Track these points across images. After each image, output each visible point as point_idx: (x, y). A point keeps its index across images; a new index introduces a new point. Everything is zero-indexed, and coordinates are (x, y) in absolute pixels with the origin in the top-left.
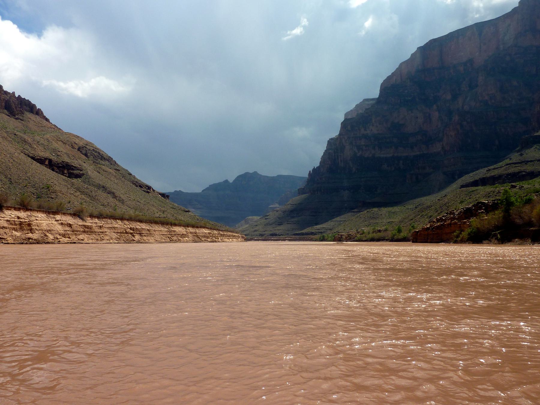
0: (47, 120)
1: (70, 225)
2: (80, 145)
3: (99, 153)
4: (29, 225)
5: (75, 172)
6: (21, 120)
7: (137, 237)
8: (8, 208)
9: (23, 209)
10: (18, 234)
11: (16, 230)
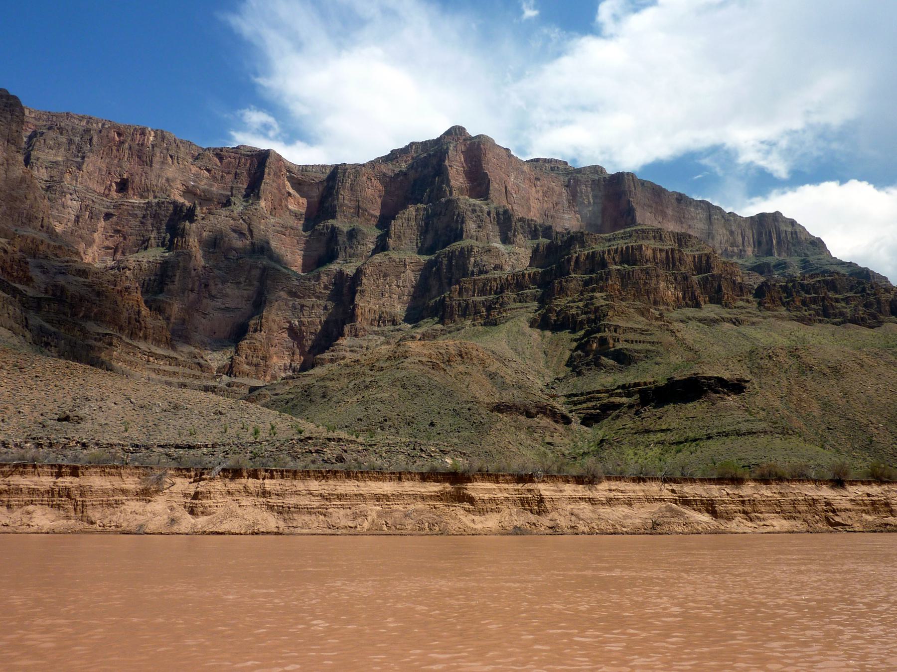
4: (887, 504)
8: (853, 483)
9: (875, 482)
10: (870, 518)
11: (868, 513)
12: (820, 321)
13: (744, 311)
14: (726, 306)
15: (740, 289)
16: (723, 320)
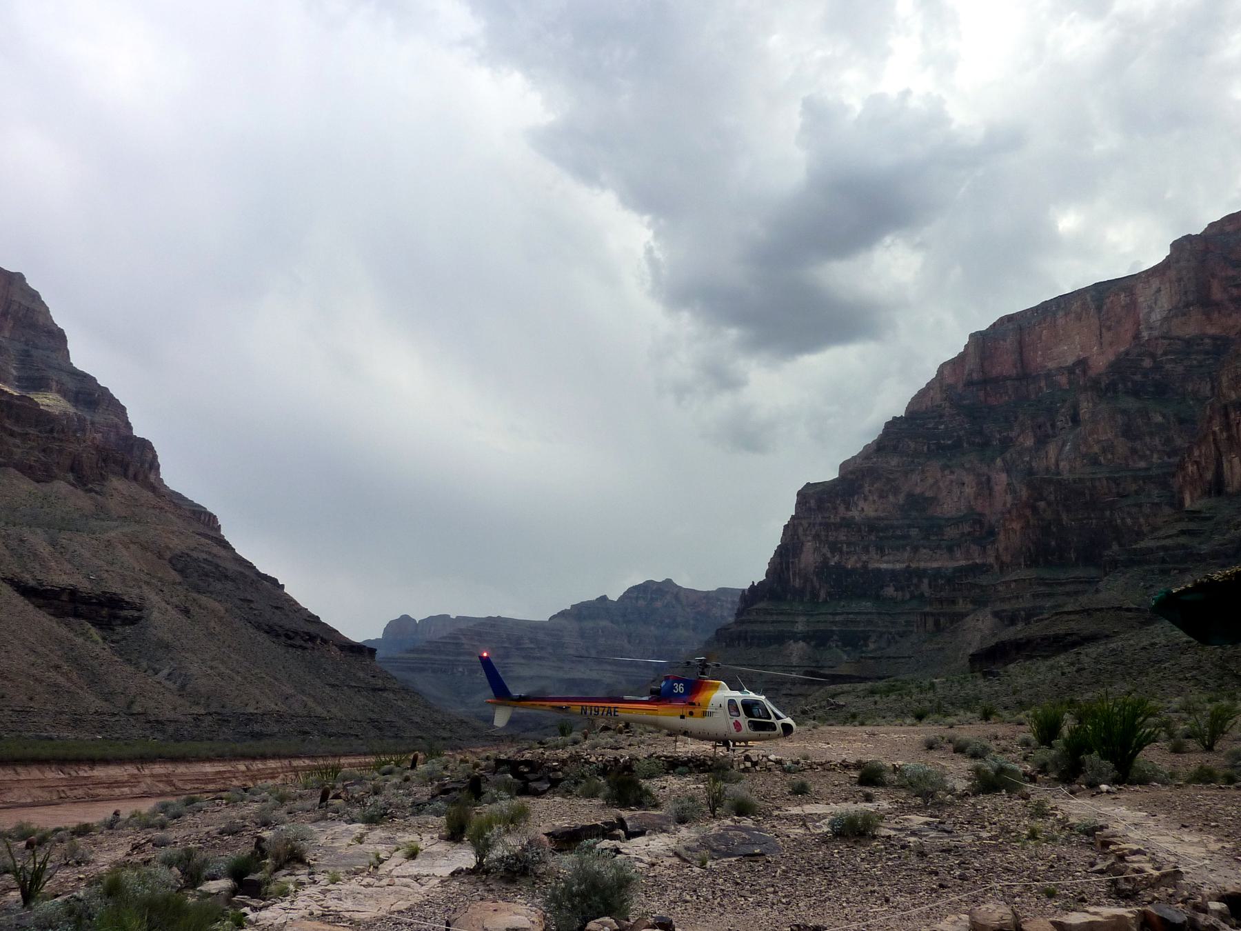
0: (157, 488)
2: (177, 552)
3: (217, 566)
5: (125, 613)
6: (96, 493)
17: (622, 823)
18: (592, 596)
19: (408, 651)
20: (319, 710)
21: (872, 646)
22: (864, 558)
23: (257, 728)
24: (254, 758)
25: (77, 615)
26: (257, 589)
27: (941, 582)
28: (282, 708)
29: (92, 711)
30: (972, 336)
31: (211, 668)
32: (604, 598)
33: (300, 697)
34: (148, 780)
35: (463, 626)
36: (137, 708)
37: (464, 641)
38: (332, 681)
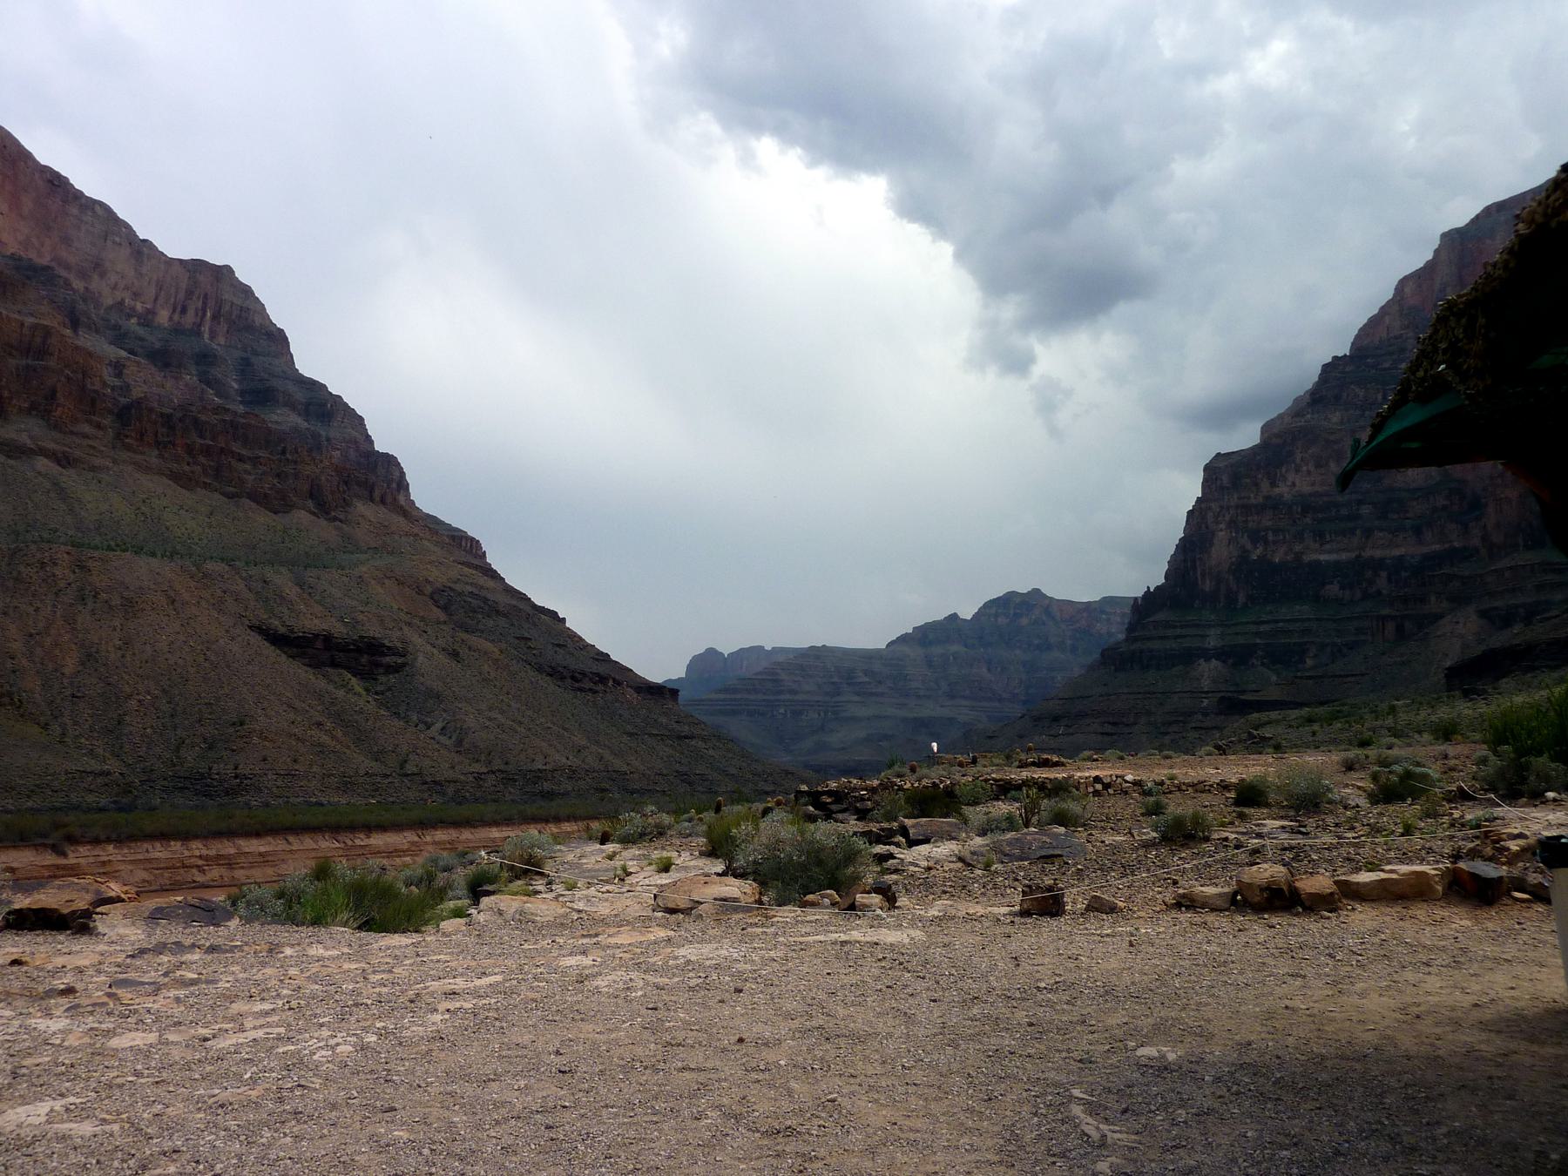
0: (409, 512)
1: (12, 870)
2: (438, 585)
3: (485, 600)
5: (387, 659)
7: (215, 873)
12: (206, 486)
13: (86, 442)
14: (56, 427)
15: (90, 402)
16: (43, 452)
17: (904, 831)
18: (940, 615)
19: (720, 691)
20: (618, 764)
21: (1309, 662)
22: (1297, 548)
23: (547, 786)
24: (547, 821)
25: (334, 664)
26: (535, 625)
27: (1404, 574)
28: (574, 761)
29: (362, 772)
30: (1444, 236)
31: (490, 719)
32: (954, 617)
33: (594, 748)
34: (430, 848)
35: (781, 659)
36: (410, 768)
37: (783, 676)
38: (629, 728)
